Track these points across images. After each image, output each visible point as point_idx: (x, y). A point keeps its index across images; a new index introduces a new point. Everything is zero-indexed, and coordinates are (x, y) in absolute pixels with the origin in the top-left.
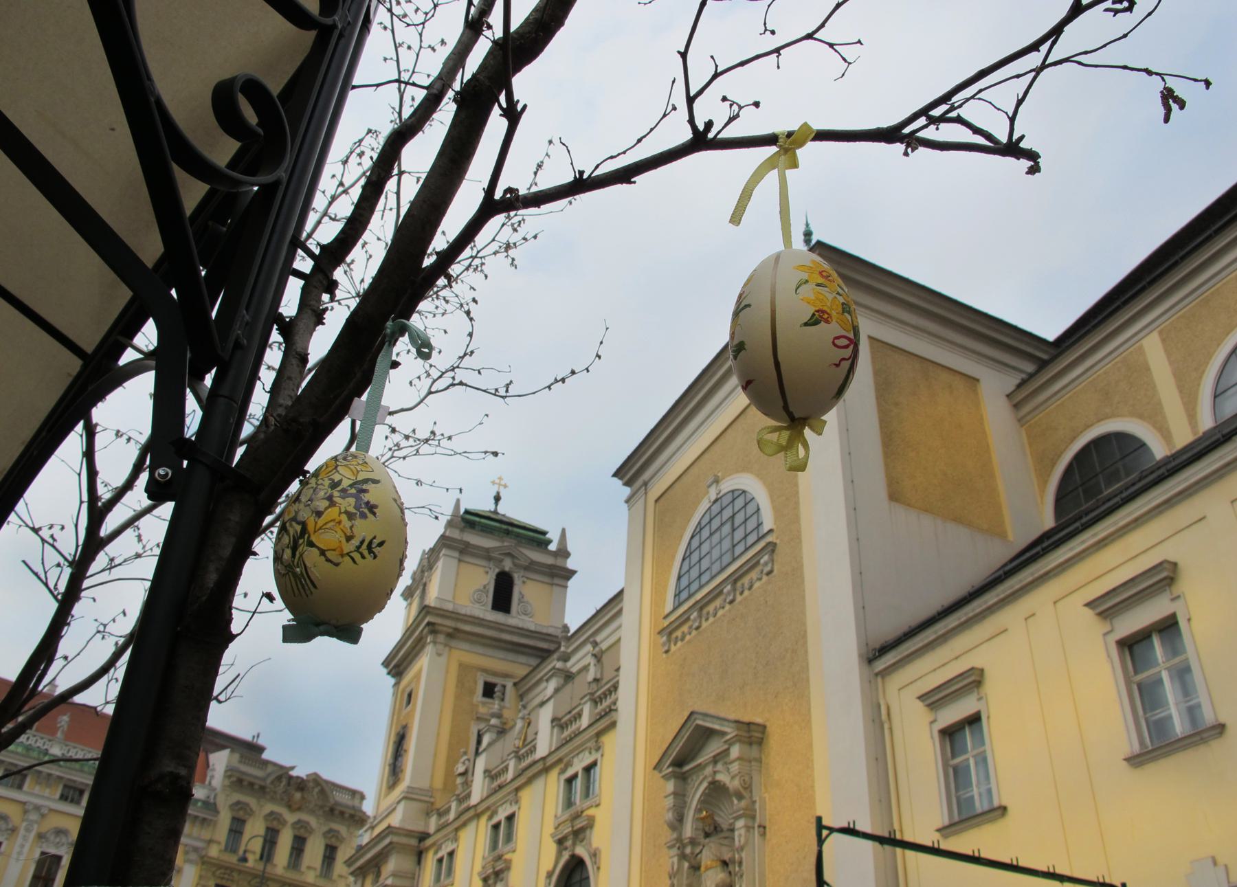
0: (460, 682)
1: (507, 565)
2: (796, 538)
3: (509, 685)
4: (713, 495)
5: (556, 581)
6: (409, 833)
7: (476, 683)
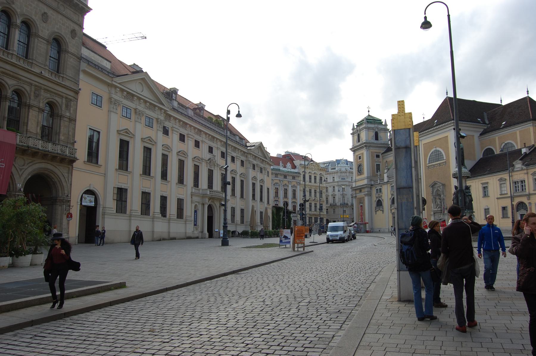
0: (372, 155)
2: (449, 162)
3: (380, 154)
4: (435, 149)
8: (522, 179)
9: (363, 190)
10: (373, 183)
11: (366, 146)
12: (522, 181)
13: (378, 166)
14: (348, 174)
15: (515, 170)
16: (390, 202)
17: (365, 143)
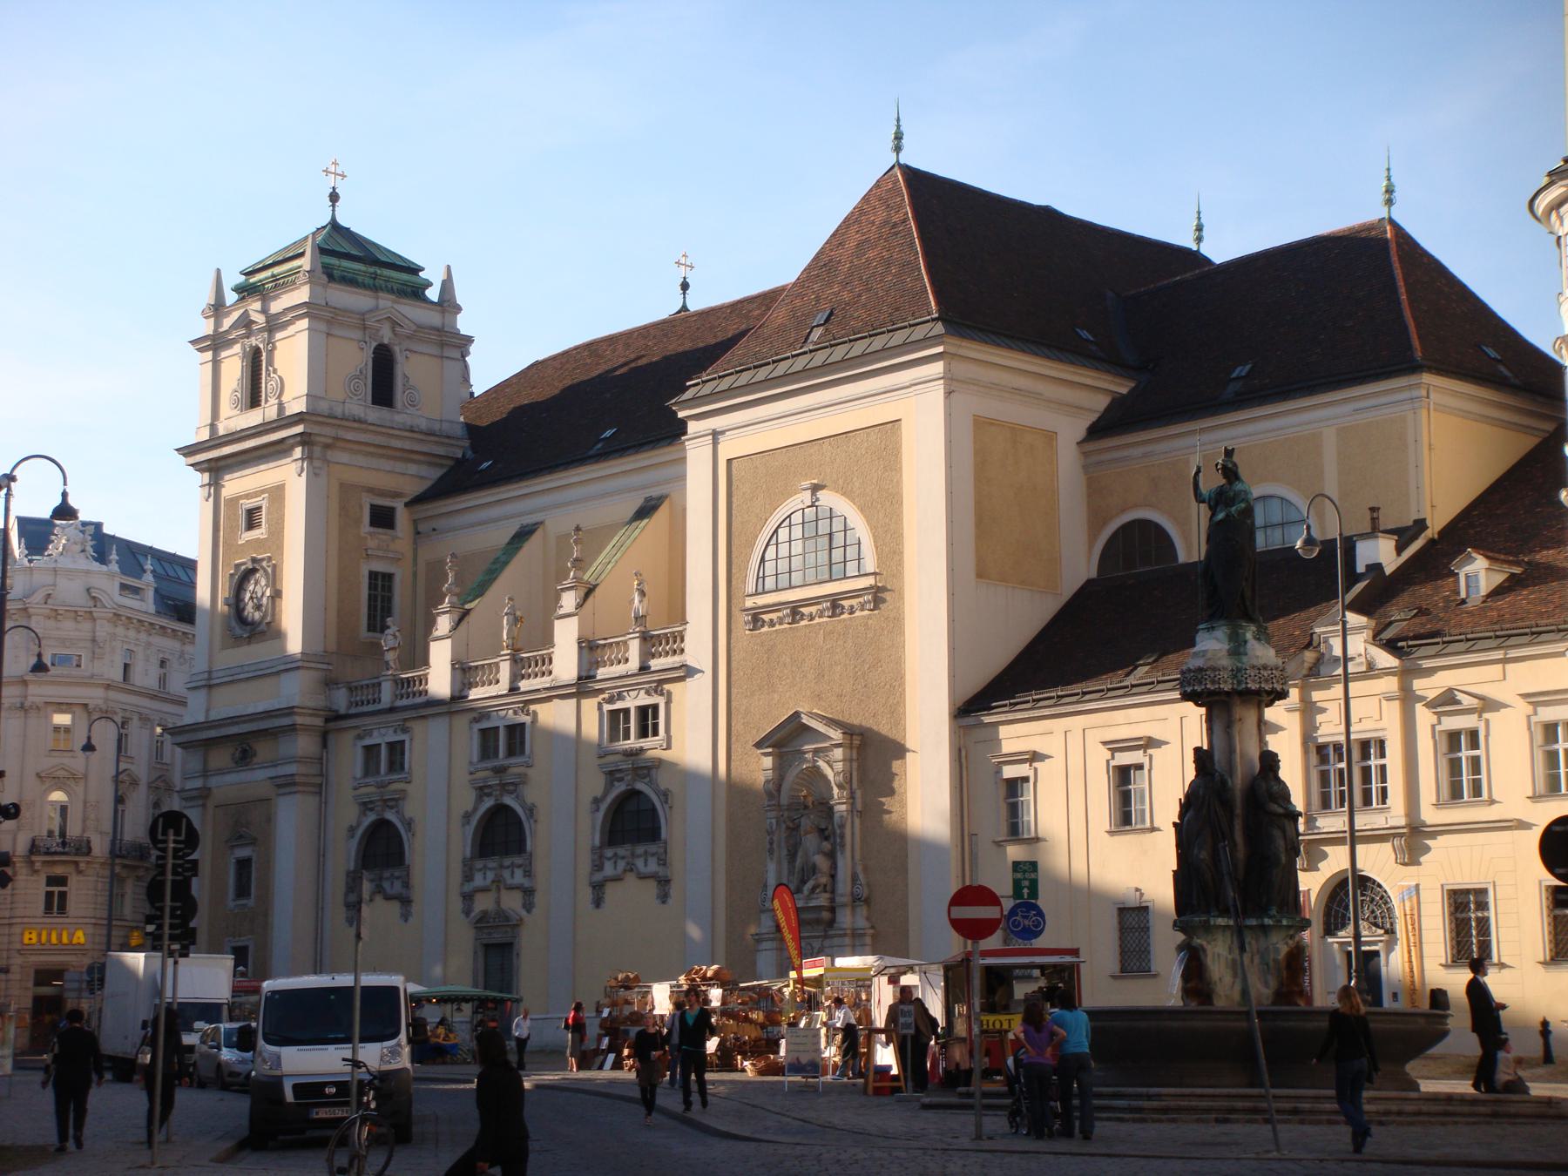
0: (344, 510)
1: (386, 336)
3: (399, 505)
5: (449, 352)
6: (315, 712)
7: (361, 507)
9: (263, 750)
10: (341, 700)
11: (305, 440)
13: (381, 584)
14: (103, 629)
16: (462, 842)
17: (298, 418)
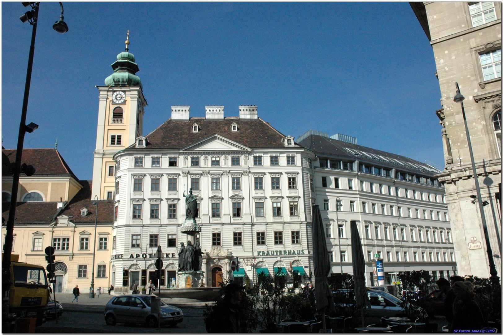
8: (66, 236)
12: (64, 239)
15: (58, 225)
